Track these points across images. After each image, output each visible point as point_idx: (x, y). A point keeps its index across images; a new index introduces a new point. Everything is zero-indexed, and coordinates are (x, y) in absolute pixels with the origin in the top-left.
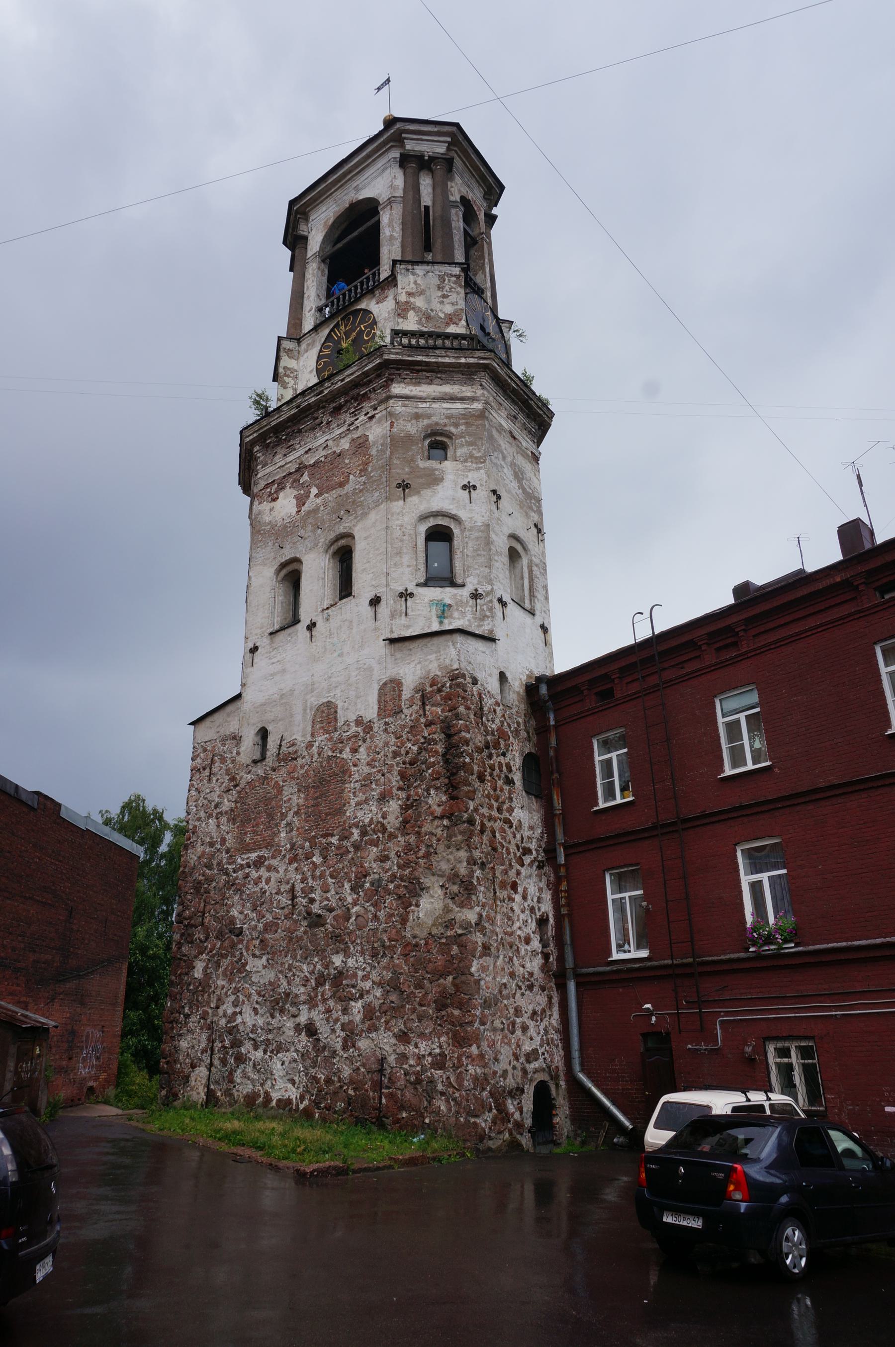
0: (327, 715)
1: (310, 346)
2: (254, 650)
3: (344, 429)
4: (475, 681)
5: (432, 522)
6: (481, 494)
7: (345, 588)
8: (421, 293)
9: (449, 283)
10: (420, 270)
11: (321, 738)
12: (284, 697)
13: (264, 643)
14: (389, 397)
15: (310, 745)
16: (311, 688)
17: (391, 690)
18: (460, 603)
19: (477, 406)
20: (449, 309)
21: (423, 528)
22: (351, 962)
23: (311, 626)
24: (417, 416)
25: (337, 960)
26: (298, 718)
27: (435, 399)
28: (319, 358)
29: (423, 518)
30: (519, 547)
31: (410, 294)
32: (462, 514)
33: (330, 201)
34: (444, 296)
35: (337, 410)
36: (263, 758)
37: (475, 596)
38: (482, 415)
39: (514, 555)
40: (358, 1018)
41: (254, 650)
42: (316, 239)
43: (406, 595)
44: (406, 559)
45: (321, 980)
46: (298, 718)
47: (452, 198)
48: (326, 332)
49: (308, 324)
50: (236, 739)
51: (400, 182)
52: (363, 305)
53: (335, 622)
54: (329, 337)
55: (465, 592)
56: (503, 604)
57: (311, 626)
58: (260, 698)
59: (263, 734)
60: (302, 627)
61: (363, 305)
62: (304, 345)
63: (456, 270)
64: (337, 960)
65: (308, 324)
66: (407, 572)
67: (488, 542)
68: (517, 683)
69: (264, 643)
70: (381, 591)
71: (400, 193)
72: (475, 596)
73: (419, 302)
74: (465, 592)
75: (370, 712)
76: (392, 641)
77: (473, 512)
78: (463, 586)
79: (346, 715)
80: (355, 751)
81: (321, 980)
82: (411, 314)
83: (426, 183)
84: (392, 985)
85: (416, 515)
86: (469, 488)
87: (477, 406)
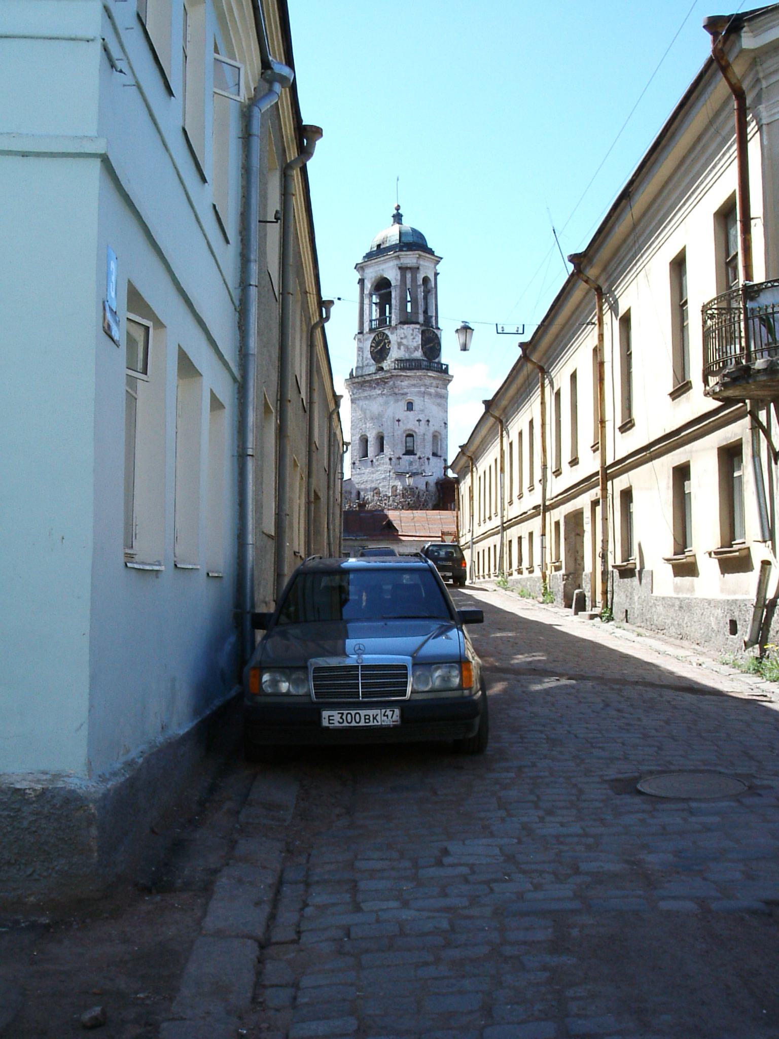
1: (367, 340)
3: (380, 392)
6: (423, 423)
7: (382, 449)
8: (406, 337)
10: (406, 326)
11: (376, 498)
13: (357, 462)
15: (373, 501)
20: (415, 344)
32: (417, 430)
35: (378, 384)
37: (420, 458)
42: (368, 285)
43: (399, 458)
48: (373, 336)
50: (351, 493)
51: (399, 277)
54: (374, 339)
61: (386, 332)
63: (418, 326)
65: (366, 329)
67: (424, 439)
71: (399, 283)
72: (420, 458)
73: (404, 341)
77: (420, 430)
83: (409, 276)
86: (419, 421)
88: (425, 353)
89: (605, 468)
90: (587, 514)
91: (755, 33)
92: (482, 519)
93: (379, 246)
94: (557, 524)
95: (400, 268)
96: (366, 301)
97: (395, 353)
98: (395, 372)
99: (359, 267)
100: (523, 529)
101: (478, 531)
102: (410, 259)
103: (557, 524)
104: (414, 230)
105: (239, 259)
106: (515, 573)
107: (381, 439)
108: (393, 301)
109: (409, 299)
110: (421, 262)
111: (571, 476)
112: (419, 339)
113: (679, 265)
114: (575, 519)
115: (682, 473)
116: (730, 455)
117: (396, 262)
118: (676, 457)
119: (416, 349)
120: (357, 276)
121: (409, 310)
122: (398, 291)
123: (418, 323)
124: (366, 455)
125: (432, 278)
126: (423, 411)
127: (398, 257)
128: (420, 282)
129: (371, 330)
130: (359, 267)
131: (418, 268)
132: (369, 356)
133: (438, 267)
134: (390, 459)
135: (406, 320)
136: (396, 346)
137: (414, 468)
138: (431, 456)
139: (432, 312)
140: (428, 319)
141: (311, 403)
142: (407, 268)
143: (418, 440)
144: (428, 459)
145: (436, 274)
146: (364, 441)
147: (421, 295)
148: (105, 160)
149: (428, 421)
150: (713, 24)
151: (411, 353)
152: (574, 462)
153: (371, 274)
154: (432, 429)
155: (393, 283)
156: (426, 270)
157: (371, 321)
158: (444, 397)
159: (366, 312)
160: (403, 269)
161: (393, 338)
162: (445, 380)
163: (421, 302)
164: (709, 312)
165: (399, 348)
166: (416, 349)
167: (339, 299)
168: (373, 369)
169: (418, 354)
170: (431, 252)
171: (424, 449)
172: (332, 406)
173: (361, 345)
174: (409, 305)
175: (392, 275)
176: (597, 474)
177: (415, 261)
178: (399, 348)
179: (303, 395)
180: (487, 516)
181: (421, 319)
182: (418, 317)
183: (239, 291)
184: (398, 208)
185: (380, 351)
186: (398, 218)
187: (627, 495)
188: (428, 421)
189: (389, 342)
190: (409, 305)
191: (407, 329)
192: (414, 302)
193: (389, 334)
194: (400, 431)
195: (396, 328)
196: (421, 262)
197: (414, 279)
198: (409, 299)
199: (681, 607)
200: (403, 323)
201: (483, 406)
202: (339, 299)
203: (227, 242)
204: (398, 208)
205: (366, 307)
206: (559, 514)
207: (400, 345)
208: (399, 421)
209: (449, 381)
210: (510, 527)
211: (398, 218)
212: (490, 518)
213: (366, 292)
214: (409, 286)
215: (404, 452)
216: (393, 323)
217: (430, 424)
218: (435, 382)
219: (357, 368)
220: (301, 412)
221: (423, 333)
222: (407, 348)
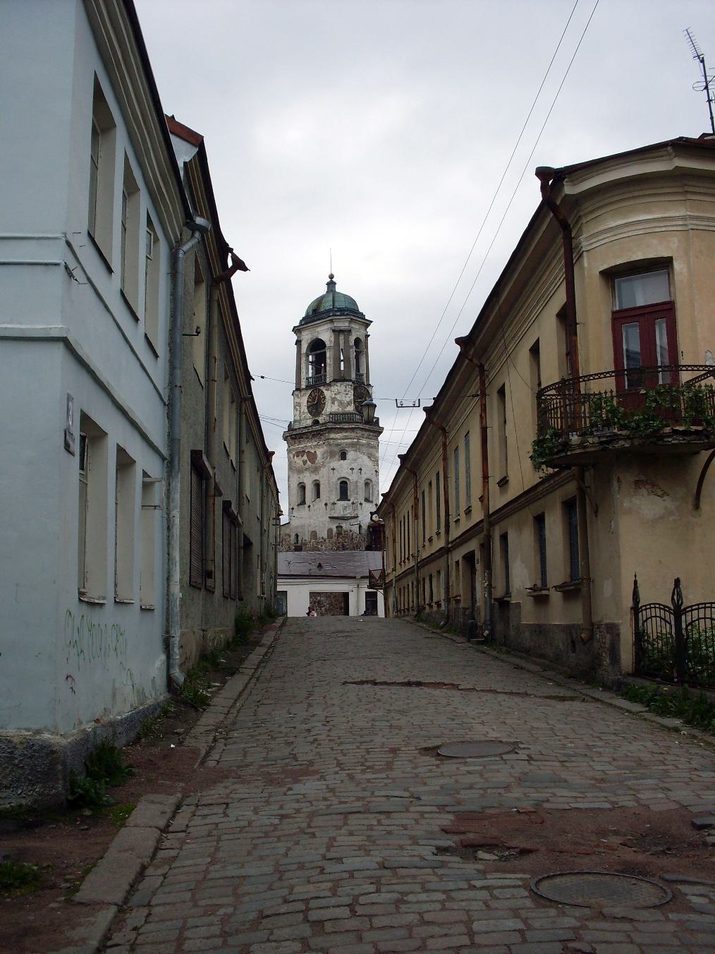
0: (314, 534)
2: (293, 509)
4: (351, 531)
5: (341, 480)
7: (318, 496)
9: (349, 388)
10: (339, 384)
12: (303, 526)
14: (328, 439)
16: (310, 525)
17: (330, 531)
18: (349, 506)
19: (355, 440)
20: (348, 399)
21: (339, 482)
22: (322, 599)
23: (309, 507)
24: (338, 445)
25: (319, 598)
26: (307, 533)
27: (343, 439)
28: (308, 401)
29: (339, 479)
30: (369, 481)
31: (335, 394)
33: (308, 331)
34: (347, 394)
36: (298, 541)
37: (353, 503)
38: (357, 444)
39: (367, 484)
40: (323, 612)
41: (293, 509)
43: (334, 504)
44: (334, 493)
45: (315, 602)
46: (307, 533)
47: (351, 344)
49: (303, 387)
50: (290, 536)
51: (333, 339)
52: (321, 388)
53: (316, 507)
54: (310, 395)
55: (350, 502)
56: (361, 504)
57: (309, 507)
58: (296, 525)
59: (297, 536)
60: (306, 506)
61: (321, 388)
62: (303, 392)
64: (319, 598)
66: (335, 496)
67: (357, 486)
68: (365, 527)
69: (295, 507)
70: (328, 502)
73: (338, 397)
74: (350, 502)
75: (326, 537)
76: (330, 517)
77: (353, 477)
78: (349, 500)
79: (319, 535)
80: (322, 546)
81: (315, 602)
82: (336, 402)
83: (342, 337)
84: (331, 604)
85: (337, 478)
86: (352, 469)
87: (355, 440)
88: (356, 408)
89: (488, 516)
90: (478, 555)
91: (574, 183)
92: (403, 559)
93: (314, 311)
94: (457, 563)
95: (334, 331)
96: (303, 359)
97: (330, 408)
98: (330, 425)
99: (297, 330)
100: (432, 568)
101: (399, 571)
102: (343, 324)
103: (457, 563)
104: (296, 344)
105: (168, 364)
106: (427, 607)
107: (317, 485)
108: (328, 361)
109: (342, 358)
110: (353, 326)
111: (465, 525)
112: (351, 396)
113: (535, 350)
114: (469, 558)
115: (540, 520)
116: (569, 506)
117: (329, 326)
118: (535, 509)
119: (349, 404)
120: (295, 338)
121: (342, 368)
122: (332, 350)
123: (350, 380)
124: (303, 502)
125: (363, 338)
126: (355, 460)
127: (332, 321)
128: (352, 343)
129: (308, 387)
130: (297, 330)
131: (350, 331)
132: (306, 411)
133: (368, 330)
134: (326, 504)
135: (340, 379)
136: (330, 402)
137: (348, 513)
138: (363, 502)
139: (363, 371)
140: (359, 375)
141: (240, 462)
142: (341, 331)
143: (350, 487)
144: (361, 504)
145: (367, 336)
146: (302, 487)
147: (353, 355)
148: (65, 341)
149: (361, 469)
150: (543, 173)
151: (345, 408)
152: (468, 512)
153: (307, 337)
154: (364, 477)
155: (328, 344)
156: (357, 332)
157: (307, 379)
158: (376, 447)
159: (303, 370)
160: (337, 332)
161: (327, 394)
162: (375, 432)
163: (353, 361)
164: (543, 398)
165: (333, 403)
166: (349, 404)
167: (263, 377)
168: (309, 422)
169: (351, 408)
170: (362, 316)
171: (357, 495)
172: (264, 460)
173: (298, 400)
174: (342, 363)
175: (326, 335)
176: (482, 521)
177: (347, 324)
178: (333, 403)
179: (233, 457)
180: (407, 557)
181: (353, 376)
182: (350, 375)
183: (167, 390)
184: (331, 277)
185: (316, 406)
186: (331, 284)
187: (504, 538)
188: (361, 469)
189: (325, 398)
190: (342, 363)
191: (339, 387)
192: (347, 360)
193: (324, 391)
194: (335, 479)
195: (329, 385)
196: (353, 326)
197: (347, 341)
198: (342, 358)
199: (540, 632)
200: (335, 381)
201: (399, 460)
202: (263, 377)
203: (156, 356)
204: (331, 277)
205: (303, 366)
206: (458, 555)
207: (333, 400)
208: (333, 469)
209: (381, 432)
210: (423, 566)
211: (331, 284)
212: (408, 559)
213: (304, 350)
214: (342, 346)
215: (339, 498)
216: (328, 381)
217: (363, 472)
218: (366, 434)
219: (295, 421)
220: (230, 471)
221: (355, 389)
222: (341, 403)
